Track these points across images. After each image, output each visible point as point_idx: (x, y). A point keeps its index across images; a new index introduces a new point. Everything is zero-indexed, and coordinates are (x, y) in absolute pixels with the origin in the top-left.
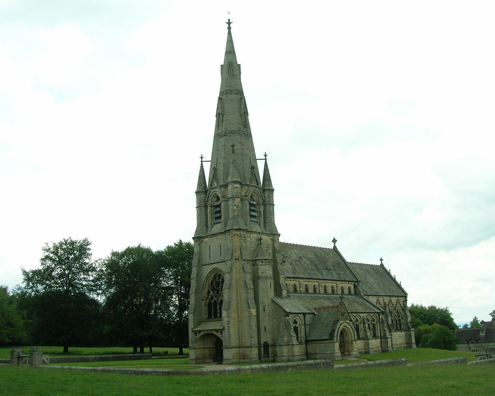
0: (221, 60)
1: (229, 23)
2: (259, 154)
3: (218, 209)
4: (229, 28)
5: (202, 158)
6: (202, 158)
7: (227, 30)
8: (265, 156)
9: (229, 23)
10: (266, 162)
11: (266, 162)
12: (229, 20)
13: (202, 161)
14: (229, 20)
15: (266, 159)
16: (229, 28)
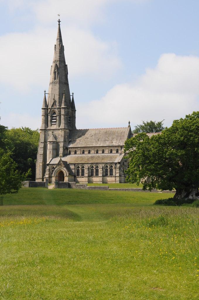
0: (55, 42)
1: (59, 22)
2: (71, 94)
3: (55, 118)
4: (59, 25)
5: (45, 92)
6: (45, 92)
7: (58, 26)
8: (73, 94)
9: (59, 22)
10: (73, 97)
11: (73, 97)
12: (59, 20)
13: (45, 94)
14: (59, 20)
15: (73, 96)
16: (59, 25)
